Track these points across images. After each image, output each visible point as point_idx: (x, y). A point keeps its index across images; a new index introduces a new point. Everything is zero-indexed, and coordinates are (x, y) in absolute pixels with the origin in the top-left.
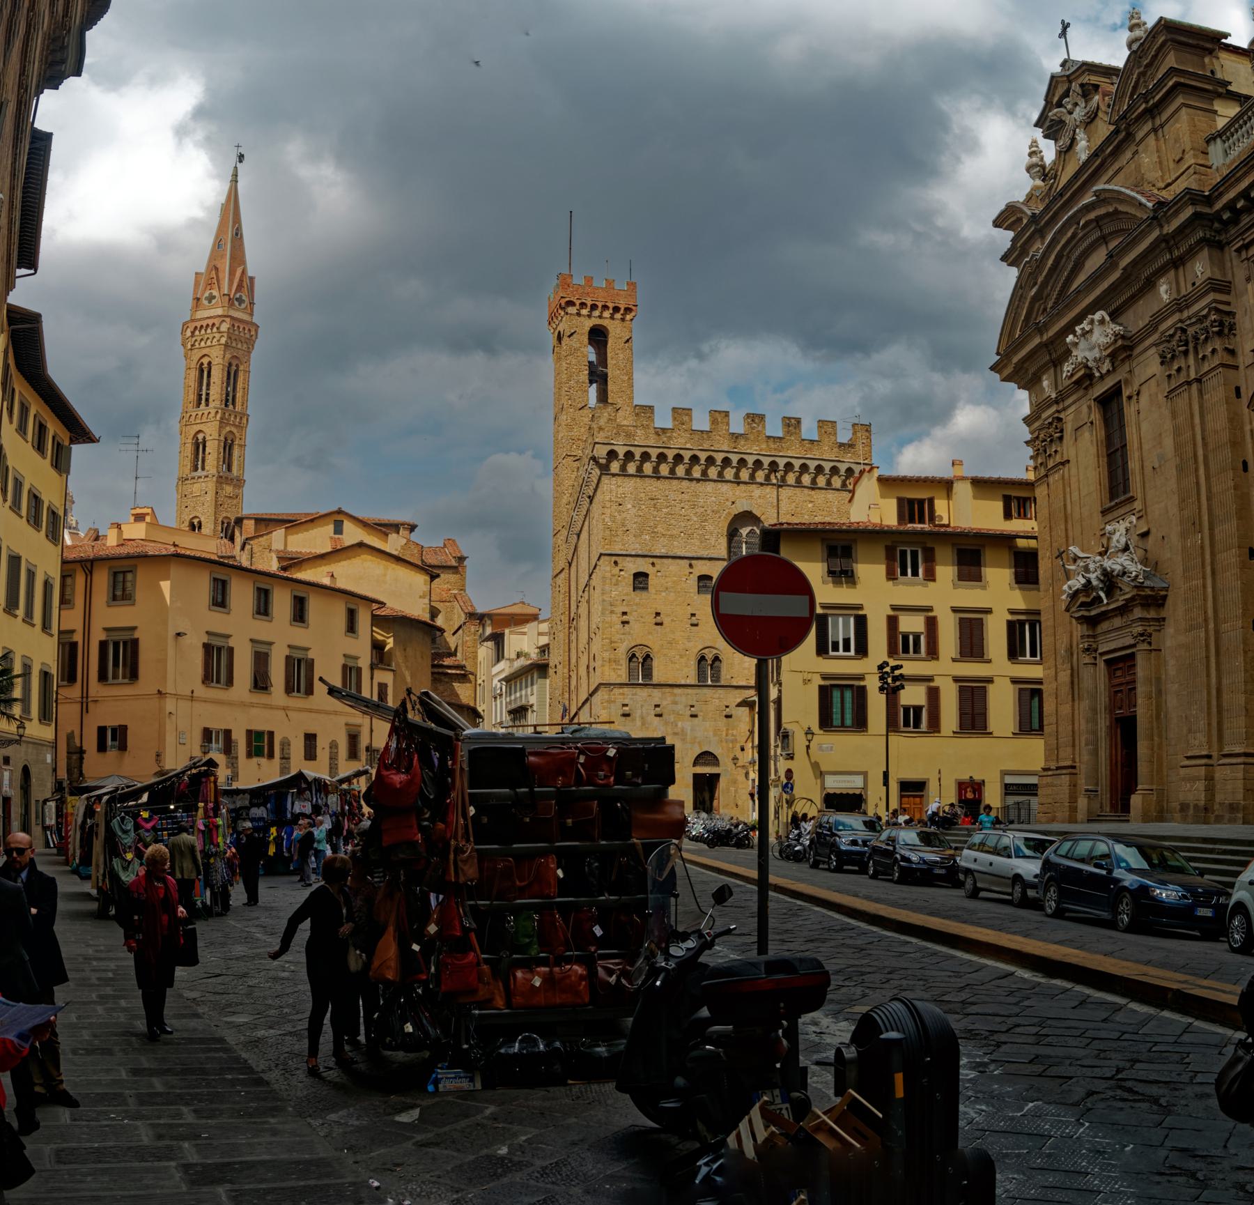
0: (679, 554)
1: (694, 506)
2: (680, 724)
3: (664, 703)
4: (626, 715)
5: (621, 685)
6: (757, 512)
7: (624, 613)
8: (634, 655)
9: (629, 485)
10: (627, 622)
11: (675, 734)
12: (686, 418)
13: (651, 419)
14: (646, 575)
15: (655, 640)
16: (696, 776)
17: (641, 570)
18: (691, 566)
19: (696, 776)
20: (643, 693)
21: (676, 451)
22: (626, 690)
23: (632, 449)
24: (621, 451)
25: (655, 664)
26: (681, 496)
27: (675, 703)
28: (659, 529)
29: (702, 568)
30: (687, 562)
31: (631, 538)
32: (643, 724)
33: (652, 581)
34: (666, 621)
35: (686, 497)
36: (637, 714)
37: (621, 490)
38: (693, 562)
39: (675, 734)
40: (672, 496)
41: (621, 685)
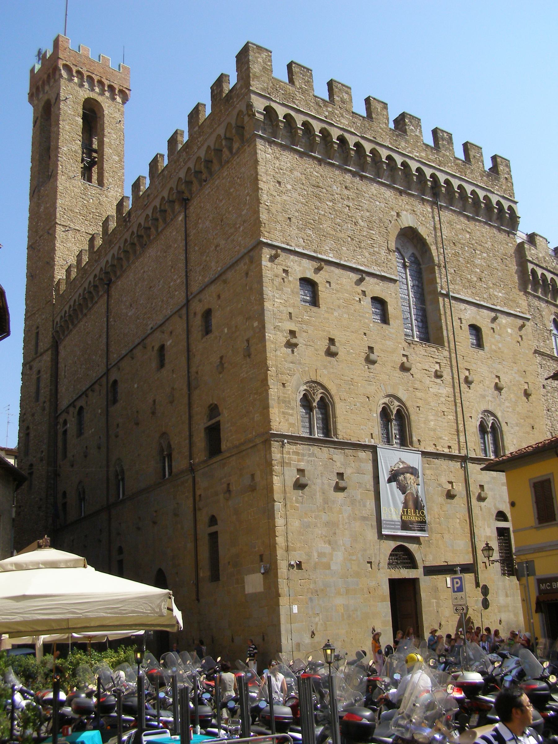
1: (359, 208)
3: (348, 472)
4: (299, 486)
5: (294, 439)
6: (422, 231)
7: (292, 333)
9: (288, 159)
10: (296, 345)
12: (346, 96)
13: (309, 83)
15: (330, 376)
16: (392, 582)
19: (392, 582)
20: (323, 453)
23: (293, 113)
24: (281, 112)
29: (375, 288)
31: (294, 231)
32: (326, 501)
33: (323, 292)
41: (294, 439)
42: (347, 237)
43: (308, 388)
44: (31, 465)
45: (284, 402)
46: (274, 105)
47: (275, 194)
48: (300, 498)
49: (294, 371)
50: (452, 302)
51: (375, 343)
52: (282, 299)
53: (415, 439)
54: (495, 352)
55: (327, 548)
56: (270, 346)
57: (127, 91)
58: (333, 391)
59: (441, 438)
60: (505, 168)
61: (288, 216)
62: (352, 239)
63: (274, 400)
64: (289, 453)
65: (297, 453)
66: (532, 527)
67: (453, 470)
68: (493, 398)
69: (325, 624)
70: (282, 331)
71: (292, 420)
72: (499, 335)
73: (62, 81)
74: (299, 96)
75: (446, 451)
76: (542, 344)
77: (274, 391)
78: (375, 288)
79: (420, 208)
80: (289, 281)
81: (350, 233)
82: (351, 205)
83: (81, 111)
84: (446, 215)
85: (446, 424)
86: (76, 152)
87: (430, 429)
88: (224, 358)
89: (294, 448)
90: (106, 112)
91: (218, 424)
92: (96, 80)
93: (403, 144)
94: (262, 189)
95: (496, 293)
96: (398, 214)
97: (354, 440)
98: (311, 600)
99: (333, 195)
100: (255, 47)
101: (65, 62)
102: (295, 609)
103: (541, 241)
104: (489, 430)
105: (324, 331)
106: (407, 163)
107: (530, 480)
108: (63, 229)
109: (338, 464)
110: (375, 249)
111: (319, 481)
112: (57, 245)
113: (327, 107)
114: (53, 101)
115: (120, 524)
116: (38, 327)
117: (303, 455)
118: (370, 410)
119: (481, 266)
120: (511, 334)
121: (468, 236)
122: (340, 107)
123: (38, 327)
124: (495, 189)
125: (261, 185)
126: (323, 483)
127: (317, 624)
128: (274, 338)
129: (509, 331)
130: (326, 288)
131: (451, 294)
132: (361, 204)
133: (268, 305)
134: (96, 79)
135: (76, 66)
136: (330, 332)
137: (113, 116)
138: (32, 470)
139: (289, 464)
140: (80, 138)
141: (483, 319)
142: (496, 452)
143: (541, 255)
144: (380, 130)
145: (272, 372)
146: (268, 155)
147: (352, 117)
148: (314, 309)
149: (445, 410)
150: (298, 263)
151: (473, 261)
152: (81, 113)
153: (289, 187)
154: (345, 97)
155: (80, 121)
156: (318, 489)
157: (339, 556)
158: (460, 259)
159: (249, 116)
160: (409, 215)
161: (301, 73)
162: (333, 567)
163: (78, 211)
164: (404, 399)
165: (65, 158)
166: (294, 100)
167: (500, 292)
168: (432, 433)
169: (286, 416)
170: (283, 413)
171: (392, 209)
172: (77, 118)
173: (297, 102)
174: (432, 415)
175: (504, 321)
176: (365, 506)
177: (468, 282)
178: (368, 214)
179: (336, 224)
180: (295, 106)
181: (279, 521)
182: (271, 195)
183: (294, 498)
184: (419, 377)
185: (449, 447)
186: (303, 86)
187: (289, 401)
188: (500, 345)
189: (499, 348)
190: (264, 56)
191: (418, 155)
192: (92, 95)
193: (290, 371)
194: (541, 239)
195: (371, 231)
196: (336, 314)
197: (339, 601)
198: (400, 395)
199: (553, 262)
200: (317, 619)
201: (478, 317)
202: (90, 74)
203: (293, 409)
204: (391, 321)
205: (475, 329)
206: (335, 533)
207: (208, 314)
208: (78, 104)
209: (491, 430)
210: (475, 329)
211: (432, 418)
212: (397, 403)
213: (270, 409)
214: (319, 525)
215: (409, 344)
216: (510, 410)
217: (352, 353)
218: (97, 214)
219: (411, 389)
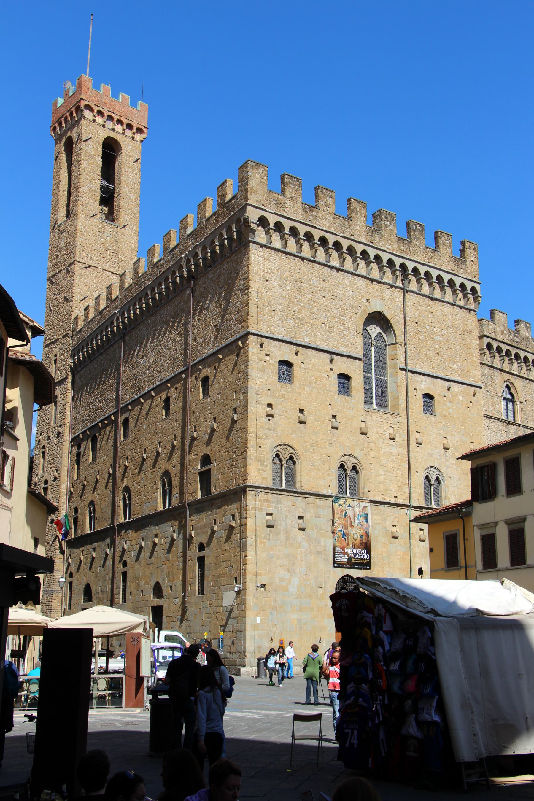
0: (321, 347)
1: (334, 297)
2: (322, 540)
6: (388, 314)
7: (270, 405)
8: (277, 456)
10: (272, 416)
11: (318, 553)
14: (289, 364)
15: (298, 440)
17: (286, 358)
18: (331, 361)
20: (287, 501)
21: (322, 233)
22: (270, 496)
23: (282, 220)
24: (272, 220)
25: (299, 468)
26: (323, 283)
27: (318, 516)
28: (303, 315)
29: (342, 366)
30: (329, 356)
32: (287, 539)
34: (309, 419)
35: (327, 286)
36: (281, 526)
37: (267, 264)
38: (335, 357)
39: (318, 553)
40: (315, 282)
42: (321, 324)
43: (280, 450)
44: (46, 482)
45: (260, 461)
46: (266, 215)
47: (263, 290)
48: (268, 536)
49: (269, 436)
50: (409, 374)
51: (338, 412)
52: (263, 379)
53: (366, 490)
54: (445, 416)
55: (287, 575)
56: (251, 416)
57: (145, 130)
58: (299, 450)
59: (388, 489)
60: (472, 252)
61: (272, 309)
62: (326, 325)
63: (252, 459)
64: (261, 500)
65: (267, 501)
66: (442, 570)
67: (397, 515)
68: (440, 456)
69: (281, 633)
70: (262, 404)
71: (264, 475)
72: (450, 402)
73: (84, 121)
74: (289, 204)
75: (393, 500)
76: (491, 409)
77: (252, 452)
78: (342, 366)
79: (388, 293)
80: (270, 364)
81: (323, 320)
82: (327, 296)
83: (100, 152)
84: (411, 298)
85: (394, 478)
86: (95, 191)
87: (380, 483)
88: (217, 419)
89: (266, 496)
90: (124, 151)
91: (209, 470)
92: (115, 120)
93: (378, 238)
94: (253, 288)
95: (451, 365)
96: (368, 300)
97: (313, 491)
98: (271, 613)
99: (312, 288)
100: (254, 164)
101: (87, 103)
102: (258, 620)
103: (501, 316)
104: (433, 482)
105: (295, 403)
106: (379, 255)
107: (444, 533)
108: (82, 267)
109: (301, 510)
110: (345, 333)
111: (283, 523)
112: (76, 281)
113: (313, 211)
114: (75, 140)
115: (126, 542)
116: (56, 356)
117: (272, 502)
118: (330, 466)
119: (440, 343)
120: (462, 401)
121: (430, 316)
122: (323, 211)
123: (56, 356)
124: (461, 272)
125: (251, 283)
126: (286, 524)
127: (275, 632)
128: (256, 411)
129: (461, 398)
130: (300, 367)
131: (409, 368)
132: (336, 294)
133: (251, 383)
134: (116, 118)
135: (98, 106)
136: (300, 404)
137: (131, 154)
138: (47, 486)
139: (261, 509)
140: (100, 177)
141: (437, 388)
142: (437, 501)
143: (498, 329)
144: (357, 228)
145: (251, 437)
146: (260, 258)
147: (334, 218)
148: (289, 386)
149: (395, 466)
150: (278, 348)
151: (433, 338)
152: (101, 152)
153: (275, 284)
154: (329, 201)
155: (100, 161)
156: (282, 529)
157: (296, 581)
158: (421, 337)
159: (246, 226)
160: (378, 301)
161: (292, 183)
162: (291, 590)
163: (95, 249)
164: (359, 458)
165: (84, 198)
166: (284, 209)
167: (455, 364)
168: (382, 485)
169: (259, 471)
170: (259, 469)
171: (363, 296)
172: (96, 158)
173: (286, 210)
174: (383, 471)
175: (456, 390)
176: (319, 543)
177: (427, 356)
178: (341, 302)
179: (313, 313)
180: (285, 214)
181: (250, 552)
182: (261, 292)
183: (263, 536)
184: (374, 439)
185: (396, 497)
186: (293, 195)
187: (264, 460)
188: (450, 411)
189: (450, 413)
190: (261, 171)
191: (390, 247)
192: (113, 135)
193: (266, 436)
194: (501, 314)
195: (342, 318)
196: (307, 389)
197: (294, 616)
198: (355, 455)
199: (511, 334)
200: (275, 629)
201: (432, 387)
202: (110, 113)
203: (266, 466)
204: (354, 393)
205: (428, 397)
206: (294, 564)
207: (205, 381)
208: (97, 143)
209: (433, 484)
210: (428, 397)
211: (382, 473)
212: (354, 460)
213: (248, 467)
214: (281, 557)
215: (368, 412)
216: (455, 467)
217: (318, 421)
218: (114, 252)
219: (366, 450)
